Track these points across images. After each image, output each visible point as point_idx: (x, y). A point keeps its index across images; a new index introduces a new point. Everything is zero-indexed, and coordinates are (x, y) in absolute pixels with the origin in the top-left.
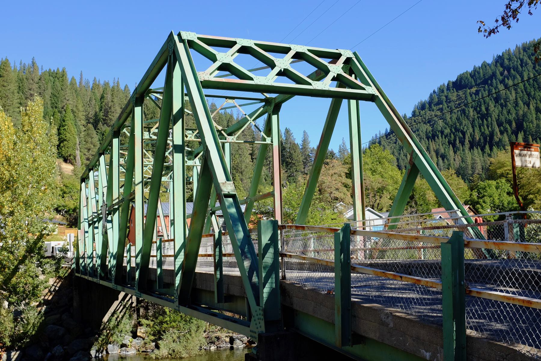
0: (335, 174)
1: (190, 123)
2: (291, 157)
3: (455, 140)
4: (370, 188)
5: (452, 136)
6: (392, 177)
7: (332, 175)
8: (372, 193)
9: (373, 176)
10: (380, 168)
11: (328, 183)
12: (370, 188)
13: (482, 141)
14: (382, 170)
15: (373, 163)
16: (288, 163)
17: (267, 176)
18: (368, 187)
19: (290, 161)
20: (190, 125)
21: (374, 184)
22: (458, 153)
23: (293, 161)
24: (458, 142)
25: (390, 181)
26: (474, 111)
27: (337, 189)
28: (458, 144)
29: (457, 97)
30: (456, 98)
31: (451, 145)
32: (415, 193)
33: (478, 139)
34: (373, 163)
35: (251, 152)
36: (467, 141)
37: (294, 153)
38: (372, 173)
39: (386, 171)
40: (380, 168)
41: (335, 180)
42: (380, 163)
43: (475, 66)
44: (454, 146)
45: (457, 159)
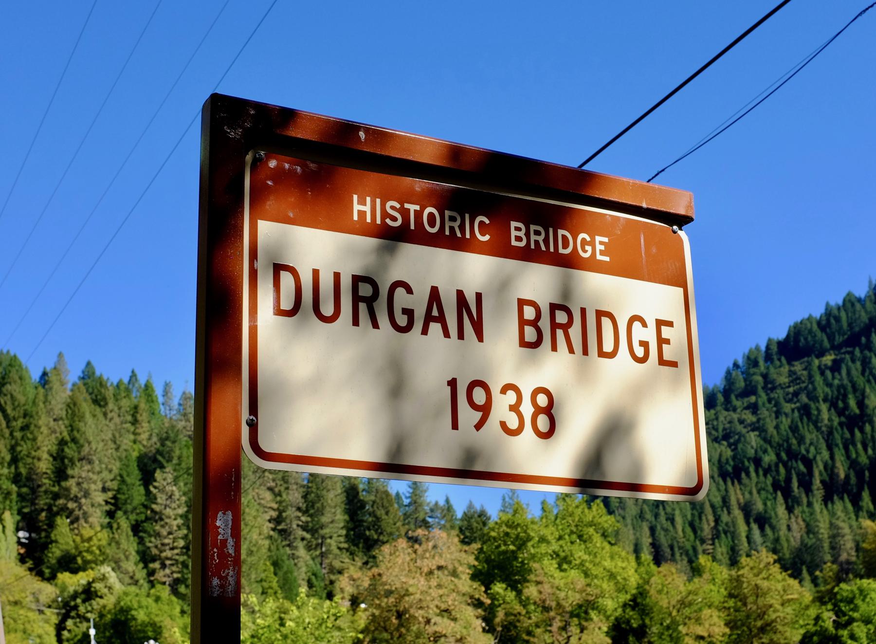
0: (440, 568)
1: (125, 441)
2: (377, 524)
3: (788, 480)
4: (554, 604)
5: (782, 470)
6: (612, 576)
7: (431, 573)
8: (559, 618)
9: (562, 574)
10: (579, 553)
11: (418, 596)
12: (554, 604)
13: (853, 480)
14: (586, 557)
15: (560, 538)
16: (370, 543)
17: (314, 574)
18: (548, 602)
19: (376, 537)
20: (123, 447)
21: (562, 595)
22: (797, 511)
23: (381, 538)
24: (795, 484)
25: (607, 586)
26: (829, 410)
27: (446, 612)
28: (796, 490)
29: (790, 376)
30: (787, 380)
31: (779, 493)
32: (647, 621)
33: (842, 475)
34: (560, 538)
35: (274, 514)
36: (817, 482)
37: (384, 517)
38: (560, 568)
39: (597, 560)
40: (579, 553)
41: (439, 586)
42: (580, 537)
43: (827, 304)
44: (787, 493)
45: (794, 526)
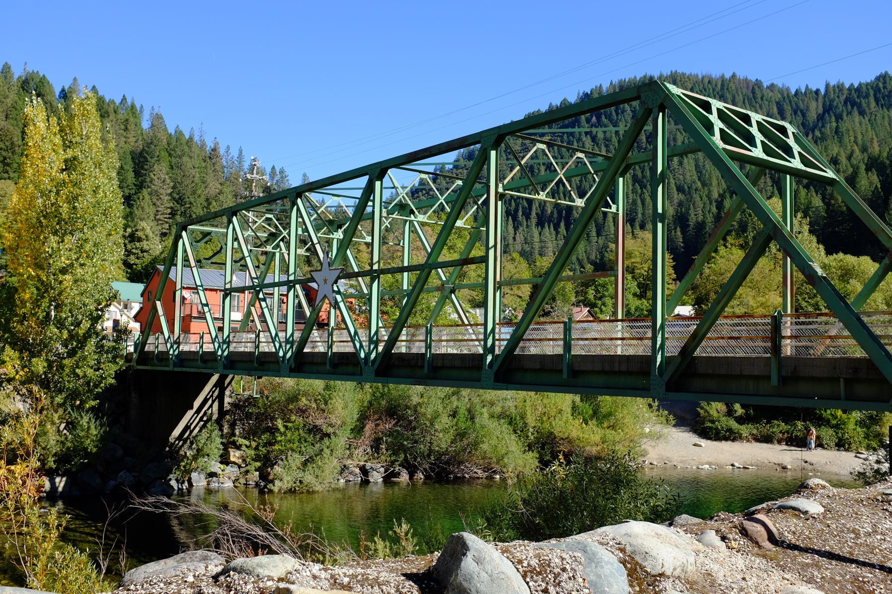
3: (516, 210)
5: (513, 204)
13: (555, 215)
22: (521, 229)
24: (520, 213)
26: (546, 170)
28: (520, 217)
29: (522, 146)
30: (520, 148)
31: (510, 217)
33: (549, 212)
36: (534, 214)
43: (551, 104)
44: (515, 219)
45: (518, 238)
